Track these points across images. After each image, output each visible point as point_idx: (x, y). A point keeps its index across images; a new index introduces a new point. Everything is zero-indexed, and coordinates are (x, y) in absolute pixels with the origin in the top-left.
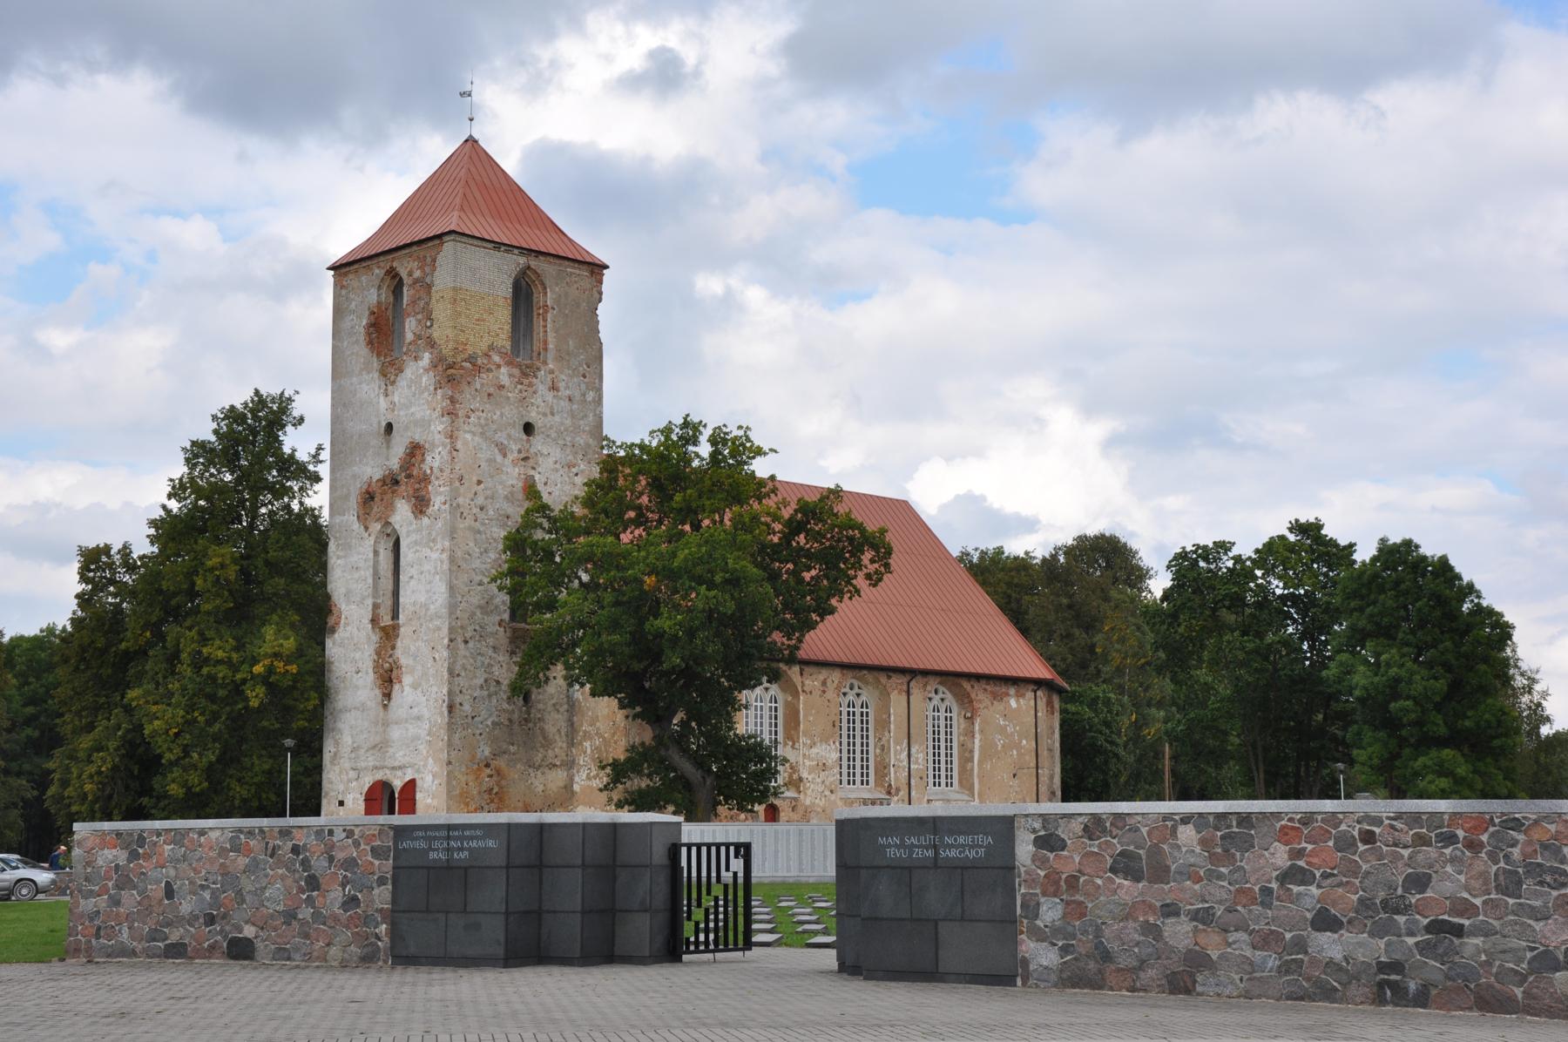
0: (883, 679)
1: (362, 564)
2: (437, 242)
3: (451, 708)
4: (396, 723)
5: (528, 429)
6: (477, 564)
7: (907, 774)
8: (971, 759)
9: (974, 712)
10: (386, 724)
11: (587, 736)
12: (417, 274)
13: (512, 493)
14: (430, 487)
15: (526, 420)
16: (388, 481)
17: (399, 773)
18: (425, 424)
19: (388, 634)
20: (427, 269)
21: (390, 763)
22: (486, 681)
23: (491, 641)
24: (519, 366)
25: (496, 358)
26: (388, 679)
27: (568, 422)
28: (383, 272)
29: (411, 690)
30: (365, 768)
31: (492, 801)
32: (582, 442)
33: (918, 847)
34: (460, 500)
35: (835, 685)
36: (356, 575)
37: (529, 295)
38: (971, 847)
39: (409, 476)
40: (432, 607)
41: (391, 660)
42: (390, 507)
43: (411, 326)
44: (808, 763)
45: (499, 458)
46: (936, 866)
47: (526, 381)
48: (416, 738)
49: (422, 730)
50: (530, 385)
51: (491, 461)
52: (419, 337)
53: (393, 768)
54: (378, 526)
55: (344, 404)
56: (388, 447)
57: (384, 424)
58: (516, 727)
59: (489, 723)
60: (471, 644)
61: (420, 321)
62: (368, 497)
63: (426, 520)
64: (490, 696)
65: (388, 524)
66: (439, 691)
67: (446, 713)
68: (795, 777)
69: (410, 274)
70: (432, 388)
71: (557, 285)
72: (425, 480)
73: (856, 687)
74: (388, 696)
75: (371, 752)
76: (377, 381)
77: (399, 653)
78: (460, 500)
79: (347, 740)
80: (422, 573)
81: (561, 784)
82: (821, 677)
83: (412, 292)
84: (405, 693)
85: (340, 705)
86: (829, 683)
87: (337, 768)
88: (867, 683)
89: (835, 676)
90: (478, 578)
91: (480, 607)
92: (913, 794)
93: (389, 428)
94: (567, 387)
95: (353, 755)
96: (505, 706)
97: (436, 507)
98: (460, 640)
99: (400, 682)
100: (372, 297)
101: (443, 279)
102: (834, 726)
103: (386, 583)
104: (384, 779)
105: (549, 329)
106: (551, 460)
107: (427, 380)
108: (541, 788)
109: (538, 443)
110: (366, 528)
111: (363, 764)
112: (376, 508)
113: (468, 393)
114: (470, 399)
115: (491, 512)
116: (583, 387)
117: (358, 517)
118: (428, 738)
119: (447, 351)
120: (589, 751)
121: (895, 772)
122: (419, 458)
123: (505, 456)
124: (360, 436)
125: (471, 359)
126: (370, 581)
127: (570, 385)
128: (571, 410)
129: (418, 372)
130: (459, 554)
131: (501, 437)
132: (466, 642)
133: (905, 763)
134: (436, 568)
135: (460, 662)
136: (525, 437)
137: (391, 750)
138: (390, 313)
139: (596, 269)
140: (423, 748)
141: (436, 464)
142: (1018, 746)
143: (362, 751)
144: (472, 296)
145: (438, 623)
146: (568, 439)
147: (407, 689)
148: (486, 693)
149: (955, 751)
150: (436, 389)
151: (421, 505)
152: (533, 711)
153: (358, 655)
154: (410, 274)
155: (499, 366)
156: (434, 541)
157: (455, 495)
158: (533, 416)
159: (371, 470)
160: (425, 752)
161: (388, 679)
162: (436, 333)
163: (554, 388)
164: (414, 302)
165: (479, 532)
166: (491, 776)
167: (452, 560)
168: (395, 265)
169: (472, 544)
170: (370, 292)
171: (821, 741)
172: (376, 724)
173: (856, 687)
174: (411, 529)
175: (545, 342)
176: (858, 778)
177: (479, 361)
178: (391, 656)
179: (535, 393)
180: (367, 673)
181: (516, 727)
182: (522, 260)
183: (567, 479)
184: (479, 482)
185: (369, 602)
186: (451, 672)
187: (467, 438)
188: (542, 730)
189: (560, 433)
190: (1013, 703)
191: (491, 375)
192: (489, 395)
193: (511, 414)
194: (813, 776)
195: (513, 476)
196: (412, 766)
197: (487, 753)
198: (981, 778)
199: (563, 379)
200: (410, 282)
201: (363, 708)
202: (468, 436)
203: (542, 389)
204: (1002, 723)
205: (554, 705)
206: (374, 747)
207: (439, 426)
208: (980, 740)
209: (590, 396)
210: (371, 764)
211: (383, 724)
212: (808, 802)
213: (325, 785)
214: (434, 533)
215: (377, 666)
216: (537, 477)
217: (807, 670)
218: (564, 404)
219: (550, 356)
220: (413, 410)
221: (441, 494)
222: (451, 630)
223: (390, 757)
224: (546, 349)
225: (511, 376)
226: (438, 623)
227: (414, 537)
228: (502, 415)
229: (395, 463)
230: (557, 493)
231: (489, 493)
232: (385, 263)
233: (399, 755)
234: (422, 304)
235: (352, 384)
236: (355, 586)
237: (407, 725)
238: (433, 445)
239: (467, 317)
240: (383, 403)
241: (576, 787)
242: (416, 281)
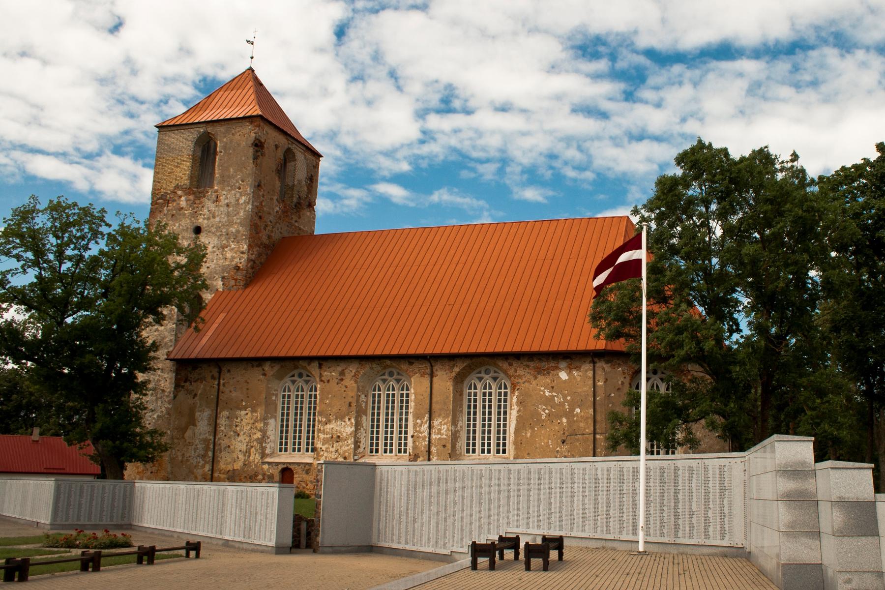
7: (427, 443)
15: (195, 225)
25: (179, 193)
32: (234, 230)
35: (353, 374)
44: (322, 436)
59: (155, 416)
64: (157, 399)
71: (225, 137)
73: (395, 374)
82: (340, 369)
86: (347, 372)
89: (352, 369)
94: (227, 198)
102: (350, 405)
116: (238, 195)
121: (414, 442)
128: (228, 212)
133: (426, 434)
142: (570, 414)
144: (166, 160)
146: (224, 230)
148: (155, 398)
155: (181, 197)
158: (202, 221)
171: (336, 419)
173: (395, 374)
179: (203, 207)
183: (221, 256)
189: (218, 228)
190: (563, 375)
191: (175, 204)
192: (173, 215)
194: (326, 446)
204: (547, 394)
208: (518, 411)
230: (213, 267)
239: (163, 173)
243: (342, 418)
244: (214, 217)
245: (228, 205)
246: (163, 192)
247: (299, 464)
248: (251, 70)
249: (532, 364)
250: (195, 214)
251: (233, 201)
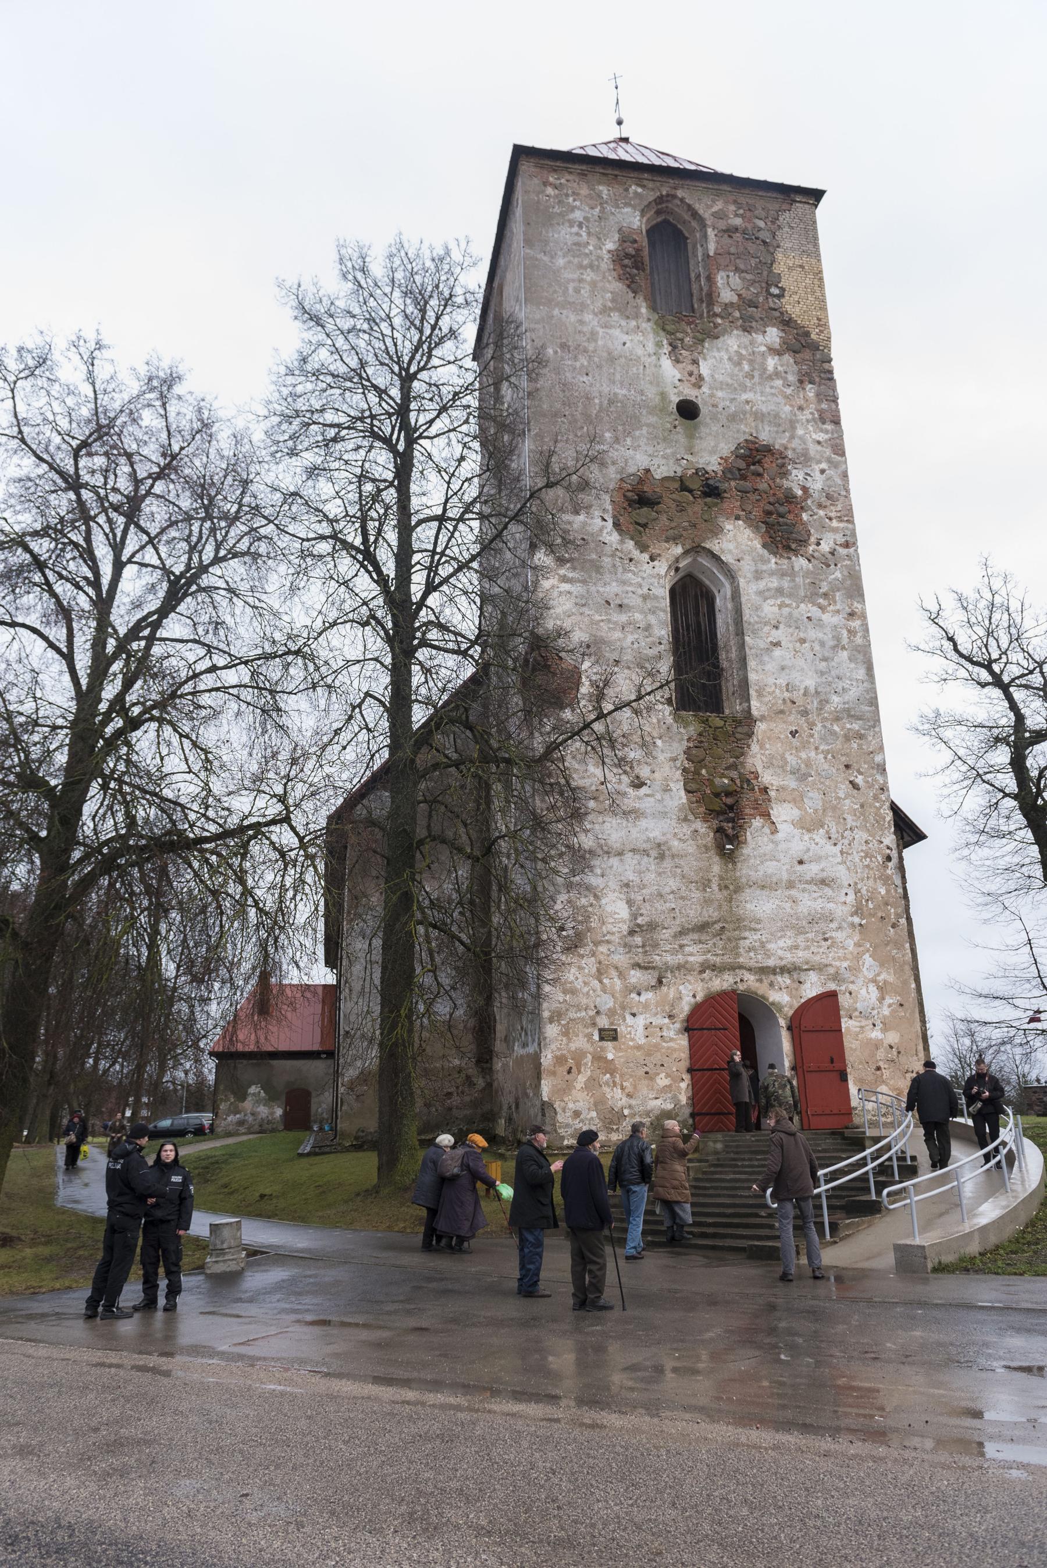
1: (635, 601)
4: (763, 887)
10: (732, 888)
14: (805, 516)
16: (696, 485)
17: (784, 980)
28: (651, 196)
29: (797, 832)
30: (679, 967)
36: (623, 618)
40: (835, 699)
41: (734, 774)
53: (764, 971)
55: (564, 346)
56: (691, 436)
63: (800, 563)
70: (792, 378)
75: (696, 936)
76: (651, 335)
77: (756, 758)
80: (803, 641)
83: (726, 240)
87: (590, 964)
95: (638, 940)
97: (825, 547)
99: (766, 815)
104: (741, 987)
110: (643, 548)
111: (669, 959)
117: (617, 525)
118: (856, 920)
124: (611, 402)
134: (838, 638)
137: (752, 938)
140: (848, 940)
141: (817, 484)
145: (856, 726)
147: (785, 829)
150: (801, 382)
160: (850, 944)
168: (680, 193)
172: (705, 884)
174: (764, 568)
178: (733, 767)
180: (667, 790)
196: (820, 968)
200: (722, 225)
201: (661, 852)
206: (703, 927)
210: (696, 959)
211: (724, 887)
214: (825, 588)
220: (745, 396)
221: (835, 530)
223: (750, 949)
226: (856, 726)
227: (774, 583)
235: (581, 322)
236: (617, 634)
237: (793, 892)
238: (805, 459)
240: (669, 370)
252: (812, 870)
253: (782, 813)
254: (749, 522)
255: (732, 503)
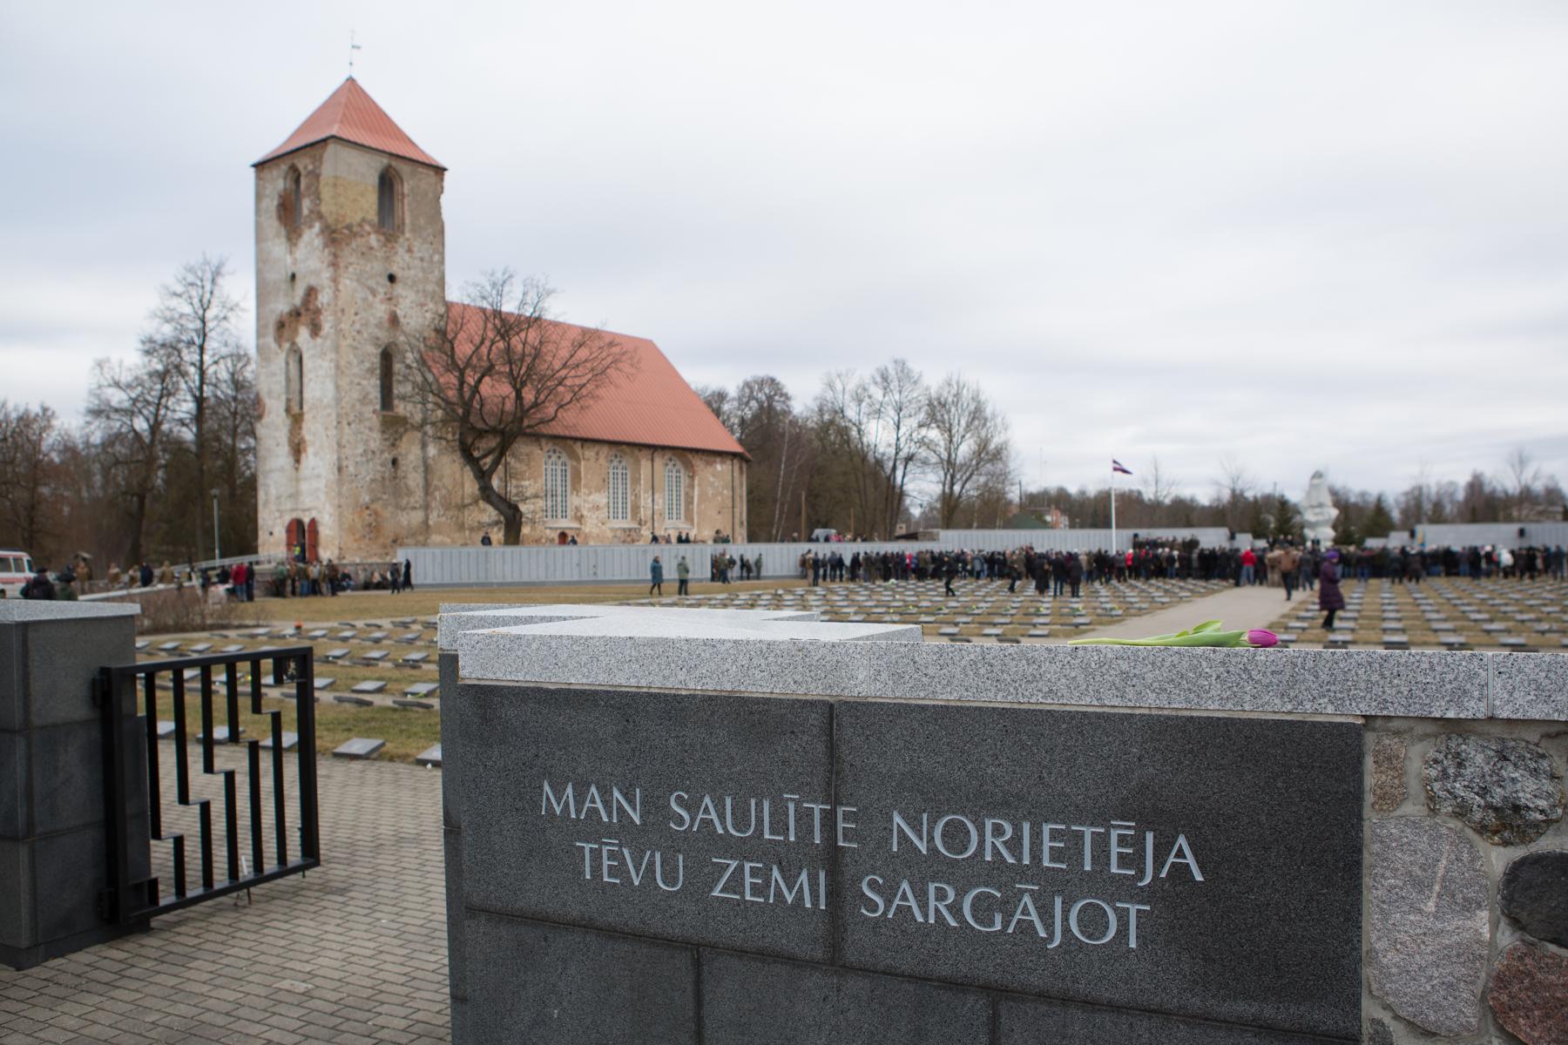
0: (636, 452)
2: (322, 144)
3: (340, 469)
5: (392, 278)
6: (356, 370)
8: (692, 503)
9: (694, 472)
10: (298, 480)
11: (437, 488)
12: (310, 167)
13: (381, 323)
17: (307, 513)
18: (317, 273)
19: (296, 419)
20: (317, 164)
21: (301, 506)
22: (365, 451)
23: (368, 424)
24: (384, 234)
25: (367, 228)
26: (297, 450)
27: (421, 275)
31: (371, 532)
33: (742, 850)
34: (343, 326)
37: (391, 186)
38: (1052, 886)
39: (307, 310)
42: (296, 332)
43: (306, 205)
44: (587, 505)
45: (370, 298)
46: (835, 962)
47: (389, 245)
48: (318, 489)
49: (321, 484)
50: (393, 248)
51: (365, 299)
52: (311, 212)
54: (287, 345)
57: (290, 274)
58: (387, 483)
59: (368, 479)
60: (353, 426)
61: (312, 201)
62: (281, 325)
63: (319, 340)
64: (368, 461)
65: (293, 343)
66: (330, 457)
67: (336, 472)
68: (579, 514)
69: (305, 168)
70: (321, 248)
72: (318, 312)
74: (298, 461)
78: (343, 326)
79: (273, 491)
81: (421, 520)
82: (596, 450)
84: (309, 459)
85: (267, 467)
86: (601, 453)
88: (625, 454)
89: (605, 450)
90: (357, 380)
91: (359, 400)
92: (656, 524)
93: (293, 277)
94: (419, 251)
96: (379, 468)
98: (345, 422)
100: (280, 185)
101: (327, 171)
103: (295, 385)
105: (407, 210)
106: (408, 301)
107: (318, 242)
108: (406, 523)
109: (399, 289)
110: (280, 346)
112: (287, 332)
113: (346, 251)
114: (348, 255)
115: (365, 335)
116: (431, 251)
119: (330, 220)
120: (438, 498)
122: (313, 296)
123: (374, 296)
125: (349, 227)
126: (284, 383)
127: (421, 249)
129: (312, 236)
130: (343, 363)
131: (372, 283)
132: (349, 424)
133: (650, 505)
135: (346, 438)
136: (388, 283)
138: (293, 197)
139: (440, 171)
140: (322, 497)
143: (283, 499)
145: (329, 411)
149: (682, 498)
151: (315, 330)
152: (399, 472)
153: (277, 434)
154: (305, 168)
155: (369, 234)
156: (325, 354)
157: (338, 322)
158: (395, 270)
159: (282, 306)
161: (297, 450)
162: (324, 209)
163: (410, 250)
164: (308, 187)
165: (356, 348)
166: (370, 515)
167: (338, 367)
169: (352, 356)
170: (278, 182)
175: (403, 219)
176: (620, 516)
177: (355, 229)
181: (387, 483)
182: (385, 161)
184: (356, 314)
185: (284, 398)
186: (339, 445)
187: (347, 283)
188: (406, 484)
190: (719, 467)
191: (363, 240)
192: (363, 254)
193: (377, 267)
195: (381, 310)
196: (315, 508)
197: (367, 499)
198: (699, 513)
199: (416, 245)
201: (282, 469)
202: (348, 282)
203: (401, 251)
205: (414, 468)
207: (327, 274)
209: (436, 258)
212: (587, 530)
213: (260, 522)
215: (291, 441)
216: (399, 312)
217: (586, 445)
218: (417, 262)
219: (407, 228)
222: (338, 415)
224: (403, 224)
225: (378, 241)
226: (329, 411)
227: (311, 352)
228: (372, 268)
229: (298, 301)
231: (364, 322)
232: (288, 161)
233: (307, 501)
234: (313, 188)
238: (323, 288)
240: (289, 259)
241: (431, 522)
242: (310, 173)
243: (599, 491)
244: (409, 268)
245: (422, 259)
246: (348, 221)
247: (571, 529)
248: (351, 80)
249: (704, 458)
250: (387, 259)
251: (427, 257)
252: (316, 472)
253: (310, 450)
254: (307, 325)
255: (303, 319)
